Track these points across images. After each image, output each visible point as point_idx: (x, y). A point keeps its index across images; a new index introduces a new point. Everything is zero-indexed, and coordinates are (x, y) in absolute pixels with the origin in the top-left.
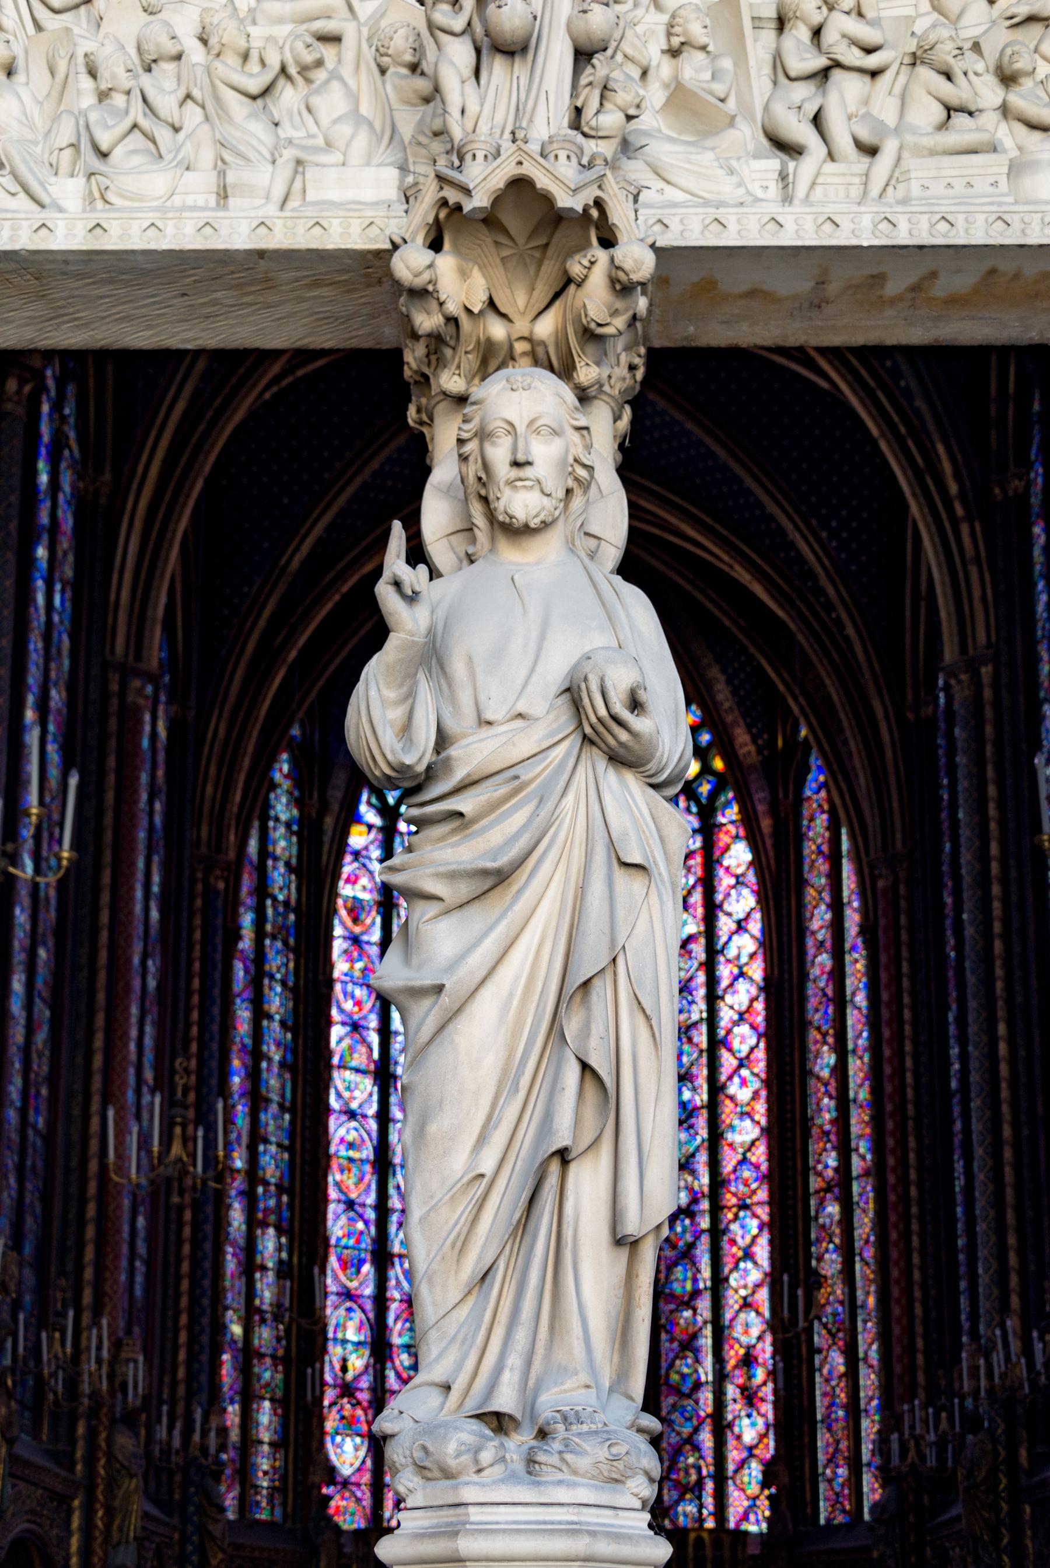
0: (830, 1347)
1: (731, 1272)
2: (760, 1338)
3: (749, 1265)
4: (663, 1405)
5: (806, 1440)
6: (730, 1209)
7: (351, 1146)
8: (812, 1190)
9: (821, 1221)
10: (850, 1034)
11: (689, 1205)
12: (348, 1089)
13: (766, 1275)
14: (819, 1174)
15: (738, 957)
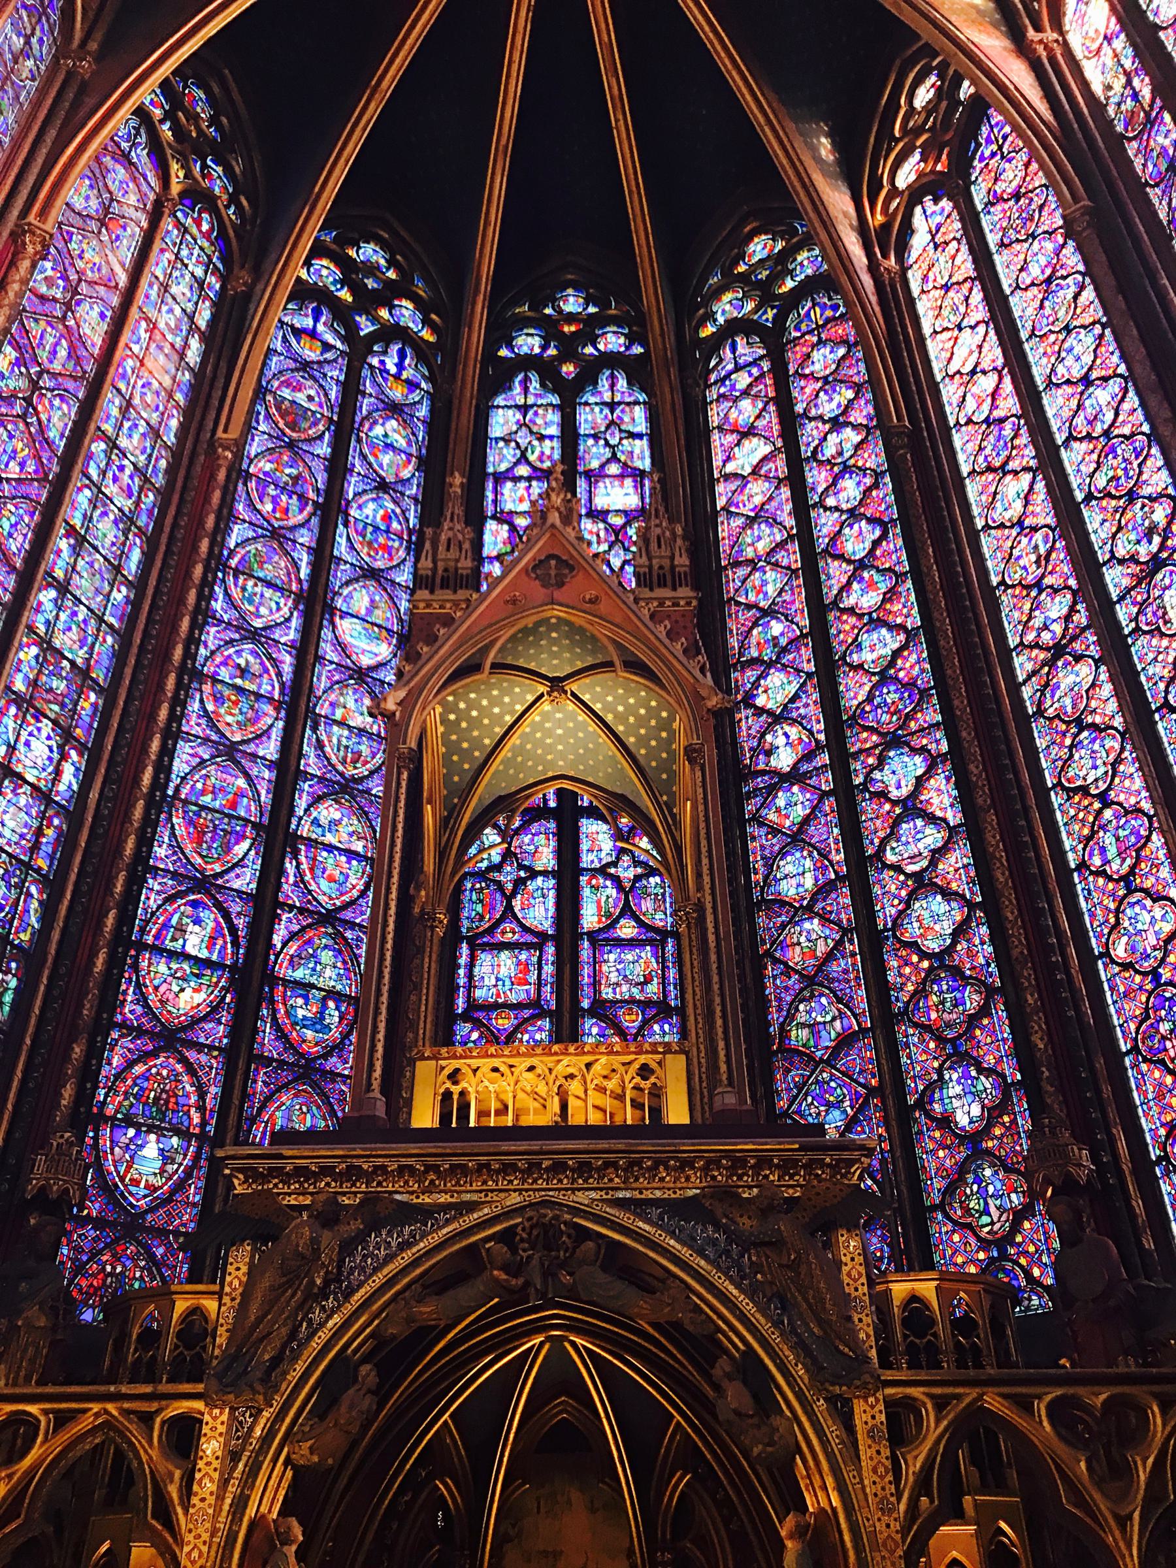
0: (1121, 903)
1: (884, 842)
2: (960, 931)
3: (919, 822)
4: (780, 1086)
5: (1107, 1091)
6: (867, 752)
7: (243, 672)
8: (1021, 680)
9: (1051, 712)
10: (1055, 425)
11: (795, 767)
12: (251, 602)
13: (953, 831)
14: (1036, 646)
15: (840, 454)
